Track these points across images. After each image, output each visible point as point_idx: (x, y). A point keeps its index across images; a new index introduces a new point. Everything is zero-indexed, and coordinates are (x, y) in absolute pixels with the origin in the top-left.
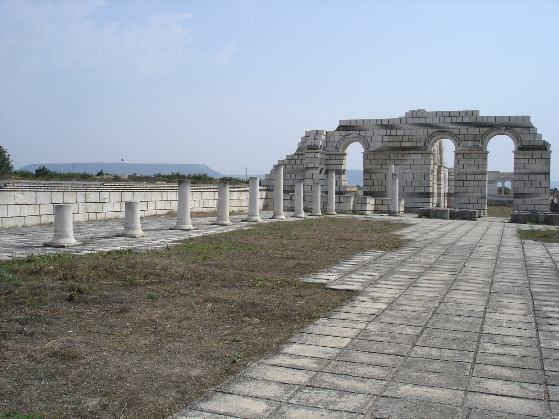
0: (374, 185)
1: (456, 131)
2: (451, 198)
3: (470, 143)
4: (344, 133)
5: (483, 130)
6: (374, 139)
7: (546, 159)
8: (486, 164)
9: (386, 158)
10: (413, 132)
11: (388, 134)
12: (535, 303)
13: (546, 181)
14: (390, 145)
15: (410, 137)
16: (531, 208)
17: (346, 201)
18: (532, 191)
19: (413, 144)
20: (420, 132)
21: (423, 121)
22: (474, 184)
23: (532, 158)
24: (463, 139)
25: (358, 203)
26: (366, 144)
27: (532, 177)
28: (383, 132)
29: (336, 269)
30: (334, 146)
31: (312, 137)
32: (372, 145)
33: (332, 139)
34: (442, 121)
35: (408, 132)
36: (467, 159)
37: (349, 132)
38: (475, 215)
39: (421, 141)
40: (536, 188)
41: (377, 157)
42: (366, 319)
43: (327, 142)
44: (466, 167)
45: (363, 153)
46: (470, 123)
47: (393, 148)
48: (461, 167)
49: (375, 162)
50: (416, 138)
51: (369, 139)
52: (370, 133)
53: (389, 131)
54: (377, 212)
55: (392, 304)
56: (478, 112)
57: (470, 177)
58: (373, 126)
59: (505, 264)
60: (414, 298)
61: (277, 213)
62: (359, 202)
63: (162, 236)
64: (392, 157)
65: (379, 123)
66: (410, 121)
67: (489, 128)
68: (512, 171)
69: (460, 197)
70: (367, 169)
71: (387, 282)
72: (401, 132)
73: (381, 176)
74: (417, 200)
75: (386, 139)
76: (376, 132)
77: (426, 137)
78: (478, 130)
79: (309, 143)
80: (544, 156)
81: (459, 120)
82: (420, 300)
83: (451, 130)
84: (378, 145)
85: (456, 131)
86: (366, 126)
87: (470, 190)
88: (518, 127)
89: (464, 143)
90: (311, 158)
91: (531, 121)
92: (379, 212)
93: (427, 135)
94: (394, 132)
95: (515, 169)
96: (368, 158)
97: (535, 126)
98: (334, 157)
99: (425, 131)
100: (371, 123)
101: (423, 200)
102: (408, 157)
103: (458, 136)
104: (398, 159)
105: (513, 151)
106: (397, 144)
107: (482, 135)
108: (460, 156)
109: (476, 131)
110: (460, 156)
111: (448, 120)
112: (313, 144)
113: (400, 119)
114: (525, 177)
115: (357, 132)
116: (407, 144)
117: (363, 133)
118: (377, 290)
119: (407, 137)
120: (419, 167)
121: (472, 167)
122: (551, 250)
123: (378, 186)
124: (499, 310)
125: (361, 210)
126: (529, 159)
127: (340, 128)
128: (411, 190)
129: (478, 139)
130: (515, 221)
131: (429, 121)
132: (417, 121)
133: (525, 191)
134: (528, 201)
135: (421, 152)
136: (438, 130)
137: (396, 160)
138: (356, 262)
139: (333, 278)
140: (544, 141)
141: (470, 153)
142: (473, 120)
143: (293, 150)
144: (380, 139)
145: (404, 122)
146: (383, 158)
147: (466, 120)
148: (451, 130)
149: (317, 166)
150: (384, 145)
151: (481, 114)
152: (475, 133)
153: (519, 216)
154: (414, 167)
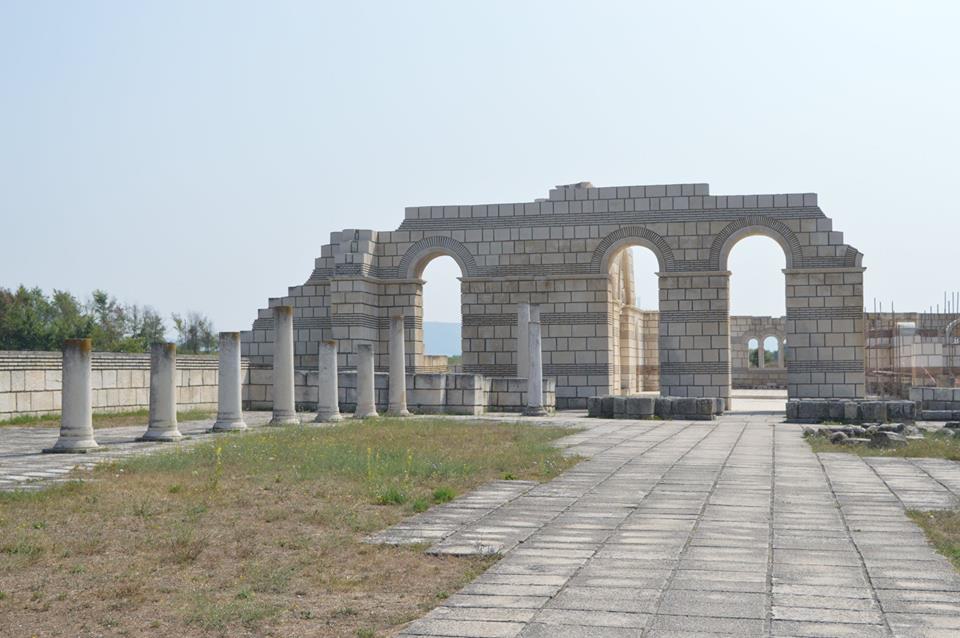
1: (660, 229)
2: (651, 377)
3: (691, 256)
4: (416, 236)
5: (717, 228)
7: (853, 285)
8: (726, 300)
10: (569, 232)
12: (868, 564)
14: (517, 261)
15: (561, 243)
16: (827, 390)
17: (428, 386)
18: (825, 355)
19: (571, 259)
20: (582, 231)
21: (587, 207)
22: (702, 343)
23: (825, 285)
25: (455, 388)
26: (464, 261)
28: (503, 234)
29: (440, 518)
30: (396, 264)
31: (345, 246)
33: (390, 250)
34: (629, 208)
35: (557, 232)
37: (428, 234)
42: (531, 604)
44: (685, 306)
48: (673, 306)
49: (487, 298)
50: (577, 245)
51: (472, 249)
52: (474, 235)
54: (496, 408)
55: (576, 576)
56: (705, 186)
57: (694, 328)
58: (480, 220)
59: (791, 498)
60: (619, 564)
61: (282, 413)
62: (458, 387)
63: (30, 466)
64: (523, 286)
65: (493, 213)
66: (561, 209)
68: (784, 314)
69: (671, 372)
70: (469, 315)
71: (557, 539)
72: (541, 233)
73: (502, 331)
74: (580, 380)
76: (488, 234)
77: (598, 242)
79: (339, 259)
80: (849, 279)
81: (666, 205)
82: (633, 568)
83: (649, 227)
84: (493, 261)
86: (466, 219)
89: (678, 255)
90: (346, 292)
91: (819, 205)
92: (501, 409)
94: (526, 233)
97: (828, 216)
99: (594, 229)
101: (593, 379)
102: (560, 286)
103: (667, 239)
104: (536, 292)
105: (783, 270)
106: (534, 259)
109: (704, 228)
110: (670, 283)
111: (642, 205)
112: (349, 260)
113: (539, 203)
114: (811, 325)
115: (447, 234)
116: (558, 259)
117: (459, 236)
118: (545, 553)
119: (555, 243)
120: (581, 308)
121: (697, 307)
122: (880, 470)
124: (797, 580)
125: (463, 405)
127: (407, 225)
128: (568, 359)
131: (601, 207)
132: (576, 208)
135: (584, 276)
136: (622, 226)
137: (533, 295)
138: (480, 503)
139: (439, 534)
140: (849, 246)
143: (302, 275)
145: (547, 210)
147: (682, 204)
149: (360, 309)
150: (505, 261)
151: (713, 192)
152: (700, 232)
154: (570, 308)
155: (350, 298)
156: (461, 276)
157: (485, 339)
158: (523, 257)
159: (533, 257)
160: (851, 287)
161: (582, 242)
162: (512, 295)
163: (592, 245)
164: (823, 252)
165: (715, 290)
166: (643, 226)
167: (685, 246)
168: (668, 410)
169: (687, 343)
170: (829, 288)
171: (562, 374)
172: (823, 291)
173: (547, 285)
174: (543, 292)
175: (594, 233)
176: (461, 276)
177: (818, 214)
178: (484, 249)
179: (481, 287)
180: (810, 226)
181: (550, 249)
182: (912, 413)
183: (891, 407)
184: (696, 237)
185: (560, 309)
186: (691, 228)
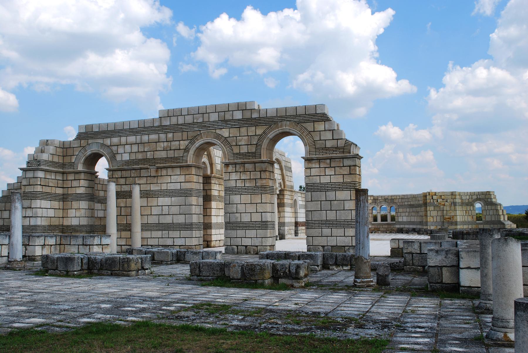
0: (121, 215)
3: (244, 150)
5: (259, 131)
6: (121, 150)
7: (350, 166)
9: (136, 175)
11: (138, 141)
13: (351, 200)
14: (140, 156)
15: (166, 144)
18: (331, 216)
19: (171, 154)
20: (178, 135)
21: (181, 121)
22: (251, 208)
24: (234, 144)
26: (112, 158)
27: (331, 195)
28: (132, 139)
32: (118, 158)
34: (206, 119)
36: (240, 172)
38: (129, 266)
39: (180, 149)
40: (337, 211)
41: (125, 174)
43: (64, 156)
44: (240, 184)
45: (107, 169)
46: (243, 120)
47: (145, 161)
48: (232, 184)
50: (175, 144)
51: (114, 148)
52: (115, 140)
53: (139, 137)
56: (253, 103)
57: (246, 198)
64: (144, 173)
65: (126, 127)
66: (166, 122)
67: (268, 126)
69: (233, 229)
72: (154, 137)
74: (176, 234)
75: (135, 148)
76: (123, 140)
77: (187, 142)
78: (254, 128)
83: (218, 131)
84: (126, 157)
85: (225, 133)
86: (111, 131)
87: (246, 218)
88: (308, 121)
89: (236, 150)
90: (30, 178)
93: (188, 140)
94: (145, 138)
95: (307, 184)
96: (114, 176)
98: (71, 177)
99: (185, 134)
100: (118, 128)
102: (164, 172)
103: (228, 139)
104: (150, 176)
105: (303, 158)
106: (149, 155)
107: (259, 136)
108: (231, 168)
109: (252, 131)
112: (36, 158)
114: (322, 196)
115: (101, 141)
116: (163, 154)
117: (108, 142)
119: (162, 144)
120: (178, 186)
121: (247, 185)
123: (127, 215)
126: (325, 168)
127: (80, 137)
128: (168, 220)
129: (255, 143)
130: (198, 276)
131: (189, 119)
132: (174, 120)
133: (323, 216)
134: (327, 231)
137: (149, 178)
141: (244, 163)
142: (248, 115)
144: (128, 147)
145: (157, 124)
146: (132, 175)
148: (218, 131)
150: (133, 157)
153: (203, 266)
154: (171, 187)
155: (32, 181)
156: (108, 167)
157: (121, 207)
158: (144, 153)
159: (149, 153)
160: (349, 168)
161: (177, 143)
162: (136, 179)
163: (183, 144)
164: (329, 144)
165: (259, 173)
166: (214, 131)
167: (240, 144)
168: (98, 266)
169: (241, 208)
170: (333, 169)
171: (165, 230)
172: (329, 172)
173: (157, 171)
174: (154, 177)
175: (185, 137)
176: (108, 167)
177: (324, 118)
178: (121, 150)
179: (118, 174)
180: (320, 126)
181: (158, 149)
182: (297, 273)
183: (278, 267)
184: (247, 137)
185: (164, 187)
186: (243, 130)
